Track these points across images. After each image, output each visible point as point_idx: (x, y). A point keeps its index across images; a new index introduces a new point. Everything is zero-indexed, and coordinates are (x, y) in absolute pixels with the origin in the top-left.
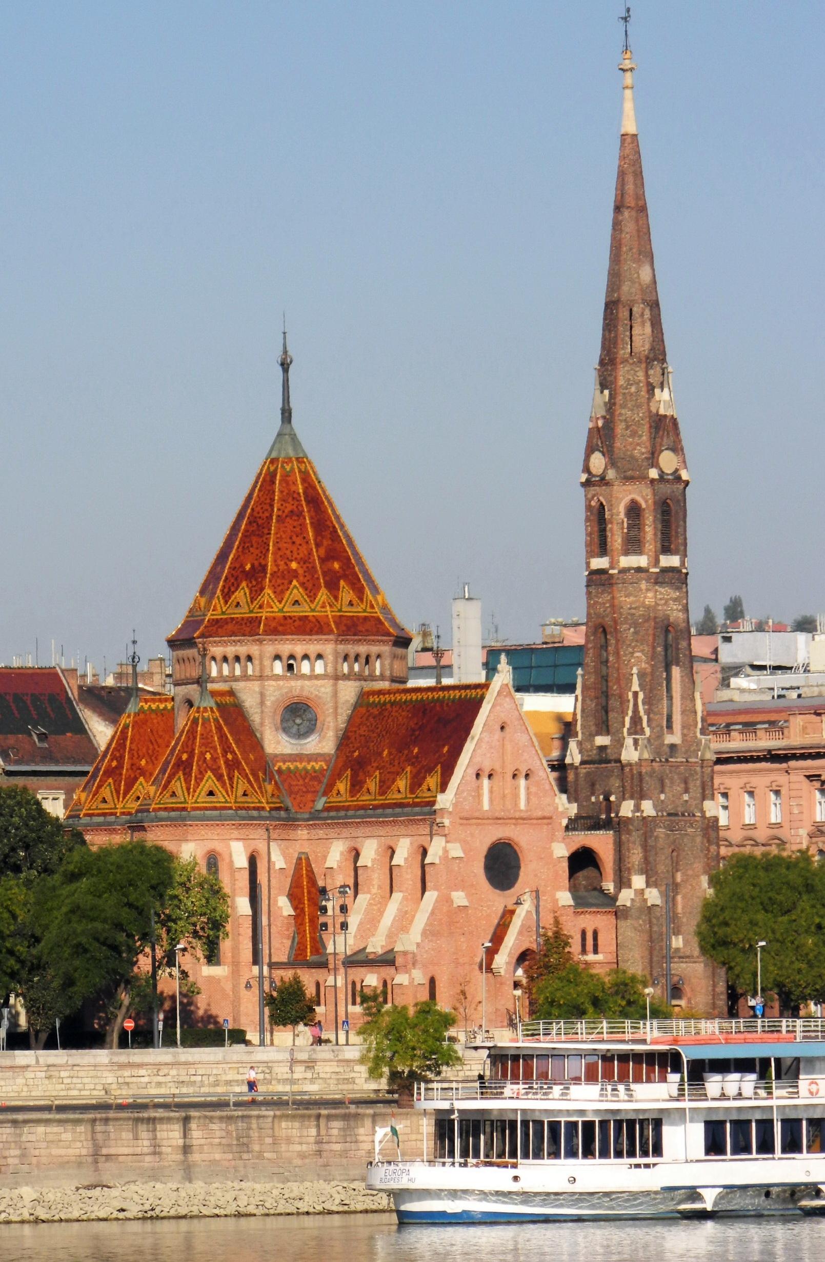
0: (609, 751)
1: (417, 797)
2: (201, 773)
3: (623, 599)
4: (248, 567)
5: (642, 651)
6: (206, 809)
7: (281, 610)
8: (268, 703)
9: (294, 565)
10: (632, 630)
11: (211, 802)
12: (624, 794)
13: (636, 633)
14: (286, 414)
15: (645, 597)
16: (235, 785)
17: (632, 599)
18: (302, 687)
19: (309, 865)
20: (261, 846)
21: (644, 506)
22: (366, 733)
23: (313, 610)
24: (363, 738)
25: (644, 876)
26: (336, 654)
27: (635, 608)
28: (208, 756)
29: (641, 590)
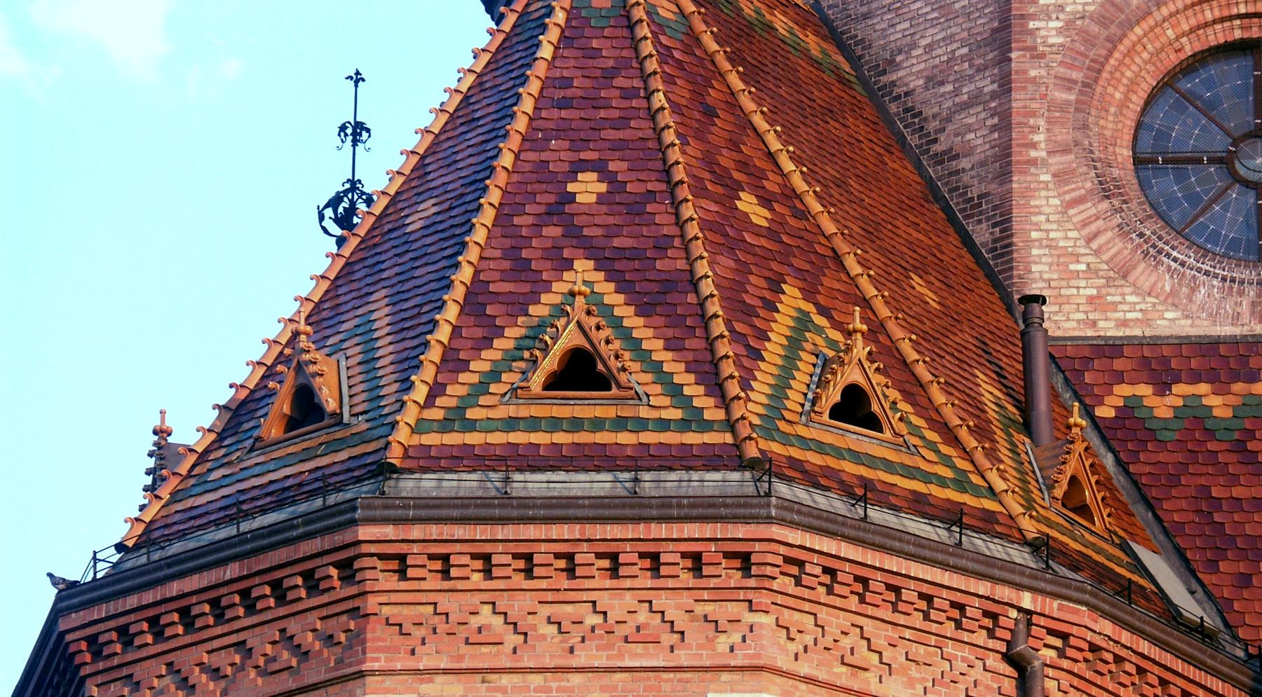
2: (520, 268)
6: (532, 461)
8: (1049, 32)
11: (576, 424)
16: (774, 349)
28: (587, 188)
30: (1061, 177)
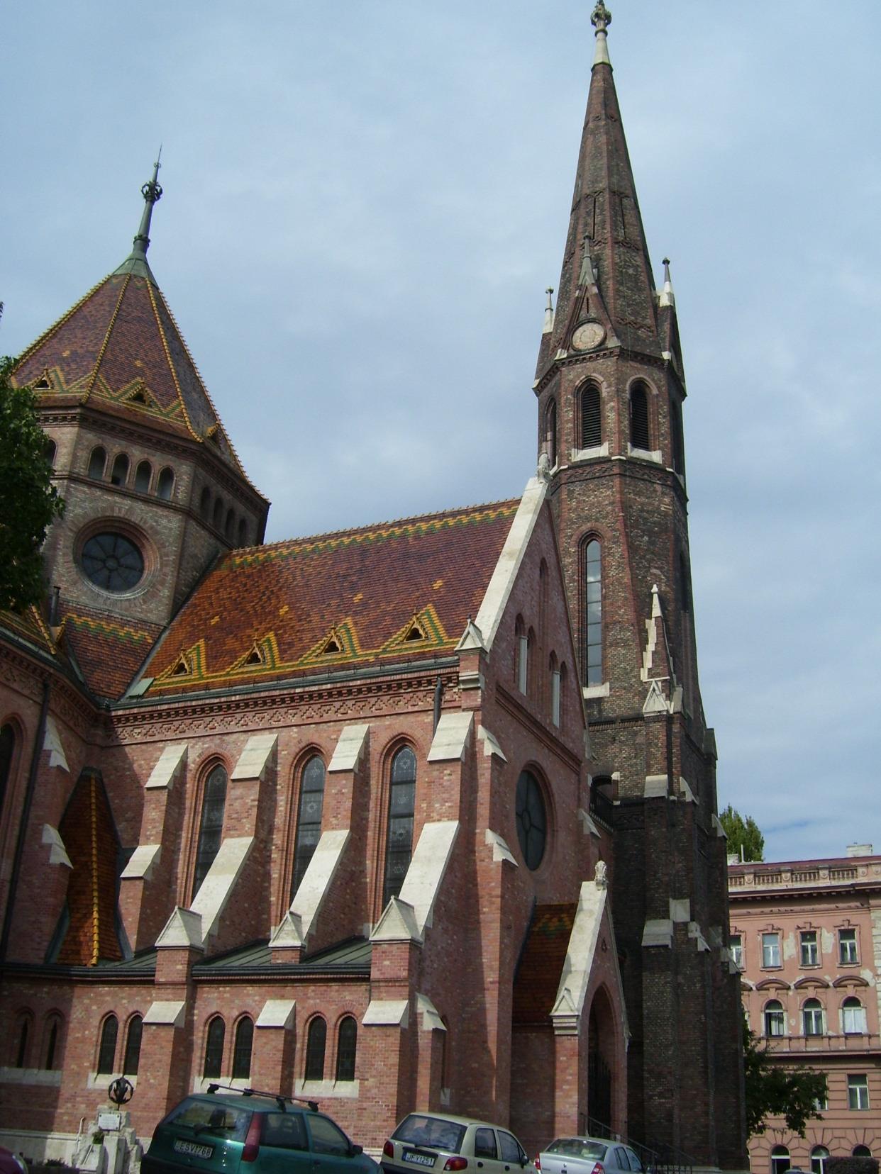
0: (606, 706)
1: (384, 651)
3: (632, 496)
4: (66, 354)
5: (660, 568)
7: (117, 399)
9: (139, 363)
10: (646, 538)
12: (649, 766)
13: (651, 543)
14: (143, 241)
15: (661, 502)
17: (643, 499)
18: (130, 510)
19: (102, 791)
20: (29, 713)
21: (655, 391)
22: (234, 595)
23: (162, 414)
24: (228, 603)
25: (687, 901)
26: (195, 479)
27: (647, 512)
29: (655, 491)
30: (64, 555)
